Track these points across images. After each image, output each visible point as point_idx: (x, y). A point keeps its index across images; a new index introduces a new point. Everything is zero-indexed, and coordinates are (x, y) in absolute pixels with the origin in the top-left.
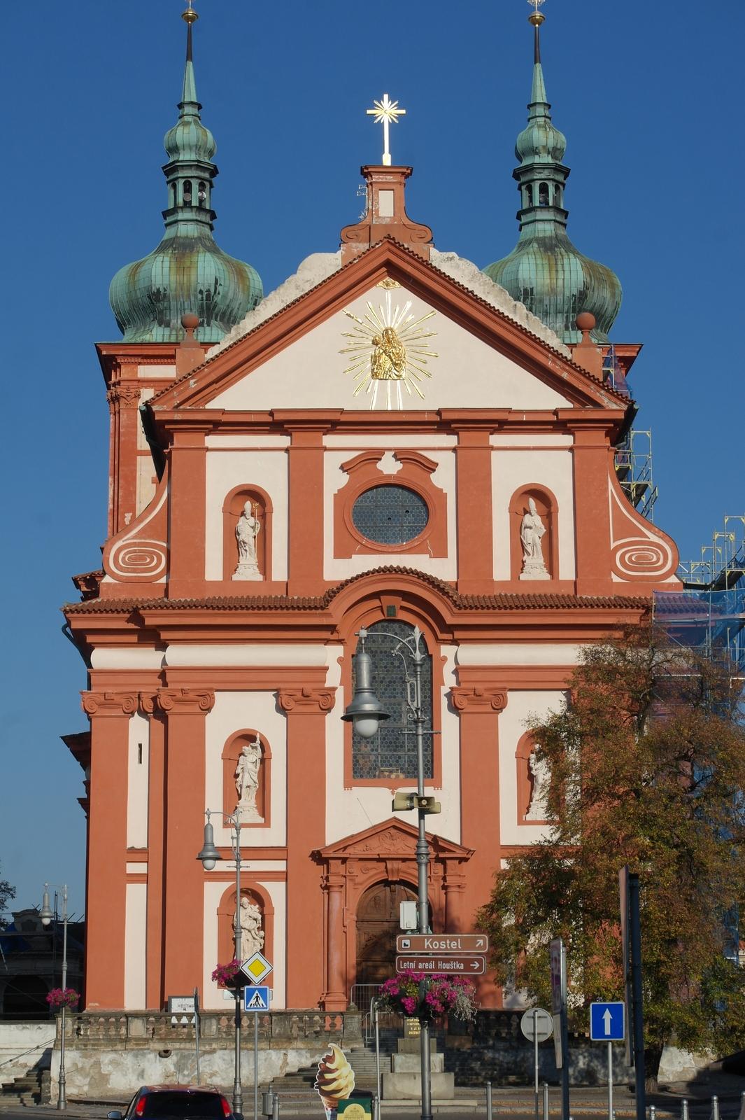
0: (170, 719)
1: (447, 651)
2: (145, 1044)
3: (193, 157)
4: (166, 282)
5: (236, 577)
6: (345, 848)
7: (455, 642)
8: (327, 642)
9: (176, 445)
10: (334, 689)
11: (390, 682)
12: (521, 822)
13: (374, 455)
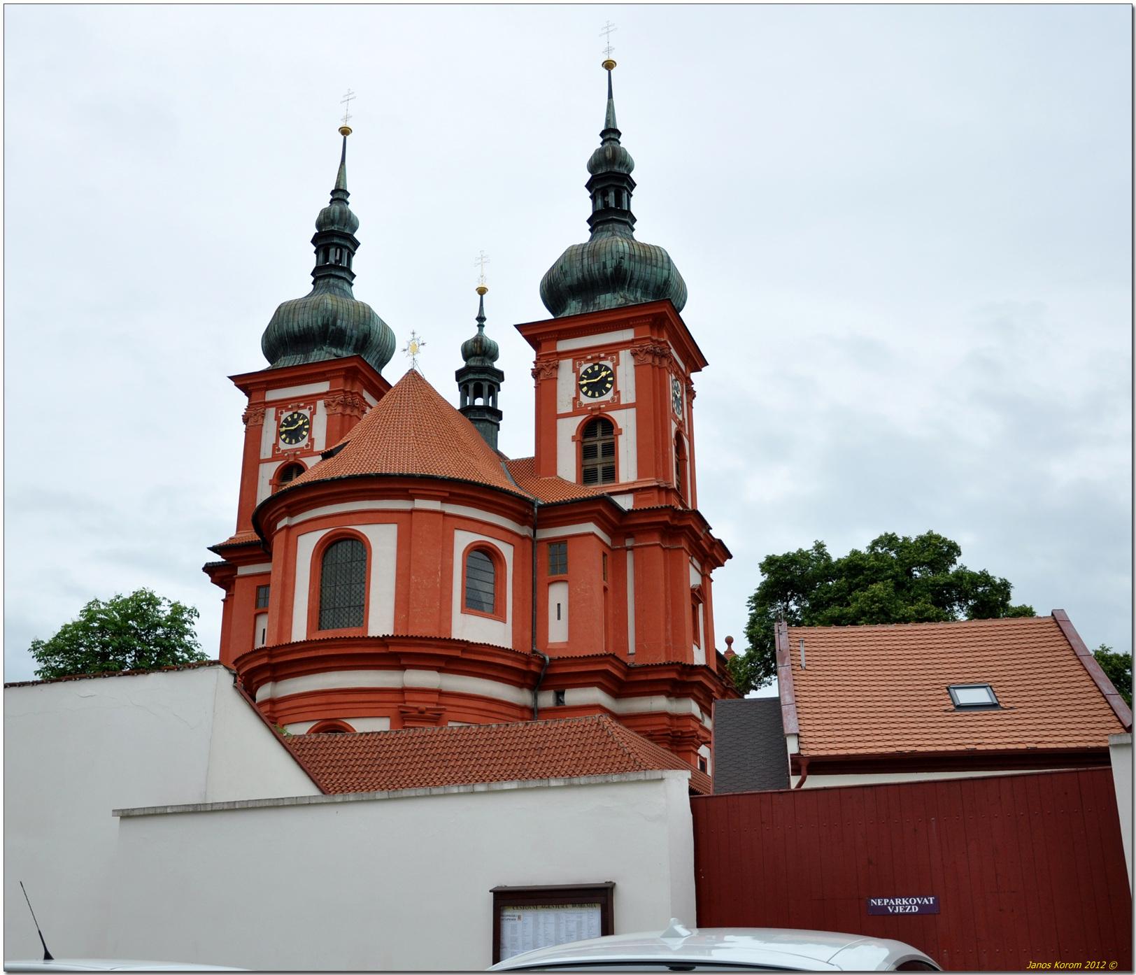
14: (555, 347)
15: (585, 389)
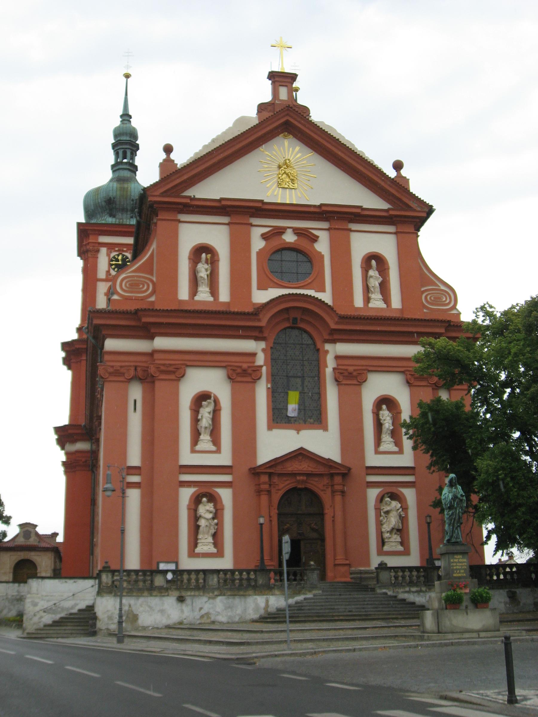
0: (158, 384)
1: (328, 347)
2: (165, 592)
3: (128, 139)
4: (115, 194)
5: (197, 298)
6: (271, 467)
7: (334, 341)
8: (257, 339)
9: (160, 217)
10: (261, 366)
11: (294, 365)
12: (377, 452)
13: (280, 231)
14: (97, 239)
15: (113, 267)
